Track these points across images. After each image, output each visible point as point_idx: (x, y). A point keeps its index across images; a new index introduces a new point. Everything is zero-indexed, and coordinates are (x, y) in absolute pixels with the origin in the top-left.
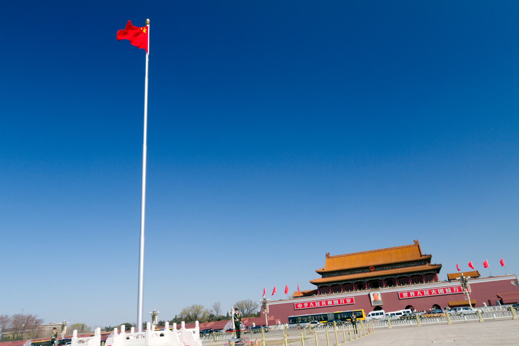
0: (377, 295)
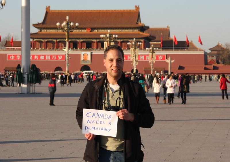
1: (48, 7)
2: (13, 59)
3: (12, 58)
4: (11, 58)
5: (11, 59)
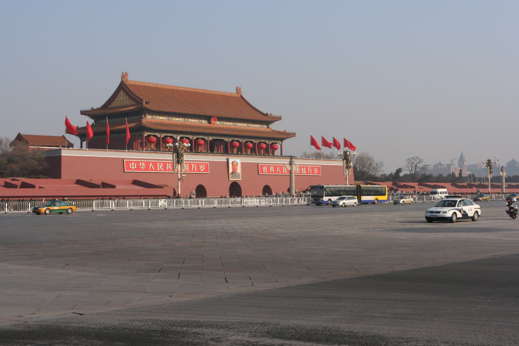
3: (133, 166)
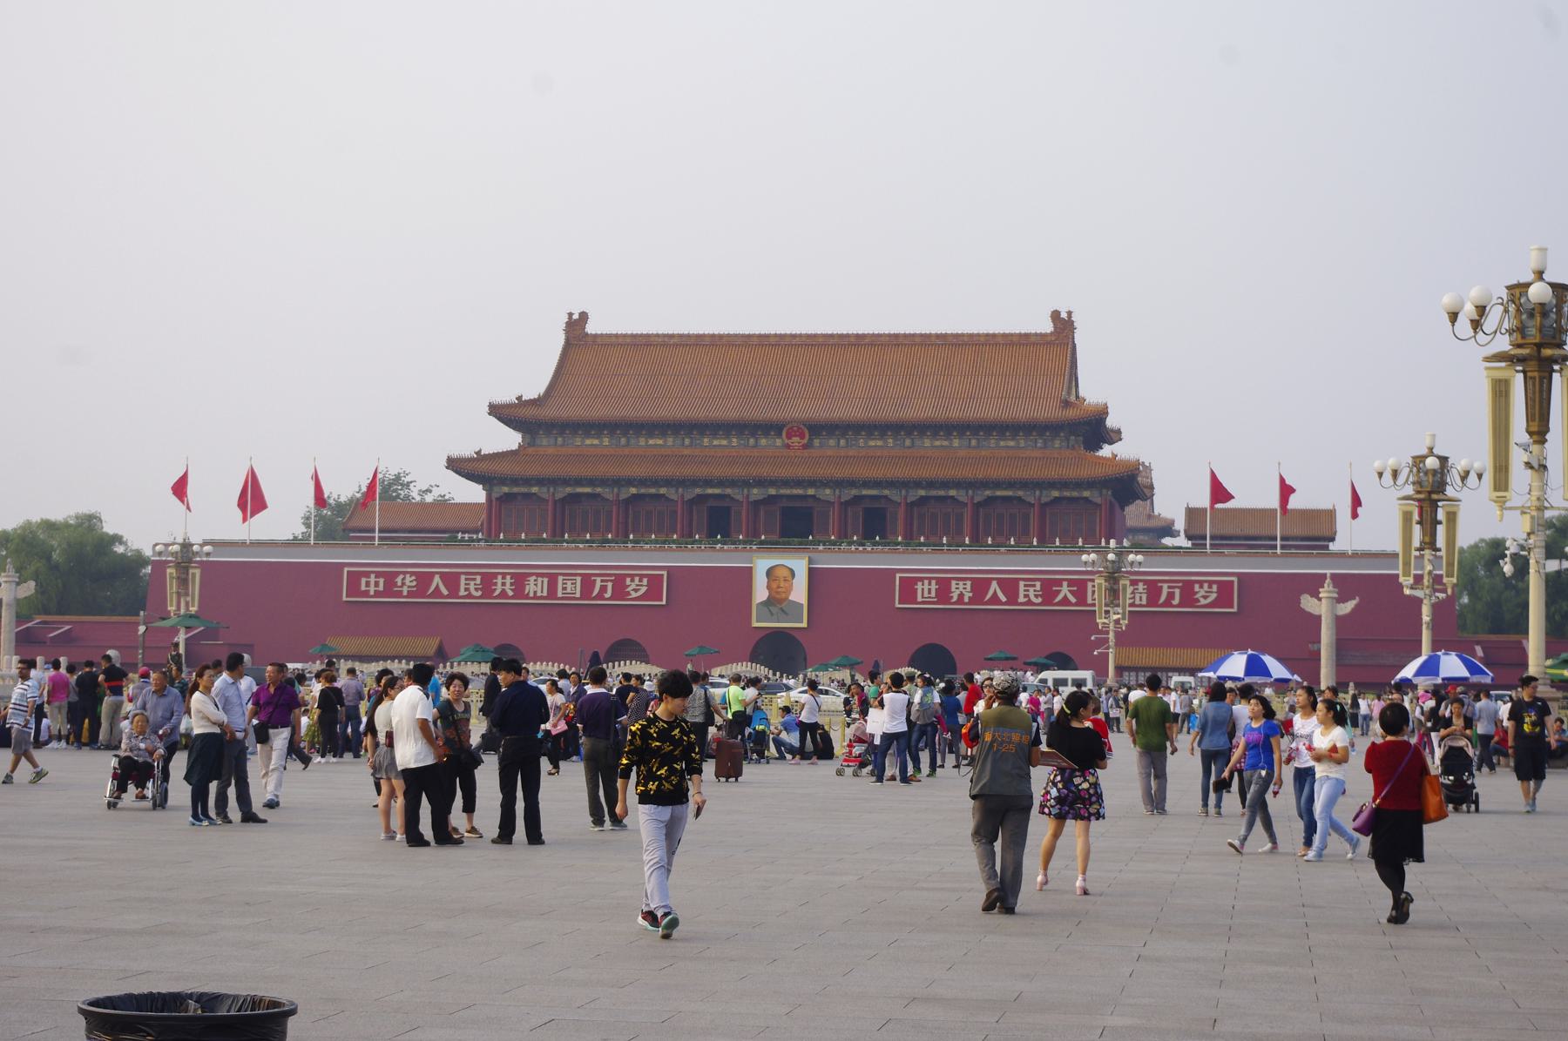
0: (780, 576)
1: (576, 317)
2: (377, 594)
3: (372, 585)
4: (363, 588)
5: (366, 594)
